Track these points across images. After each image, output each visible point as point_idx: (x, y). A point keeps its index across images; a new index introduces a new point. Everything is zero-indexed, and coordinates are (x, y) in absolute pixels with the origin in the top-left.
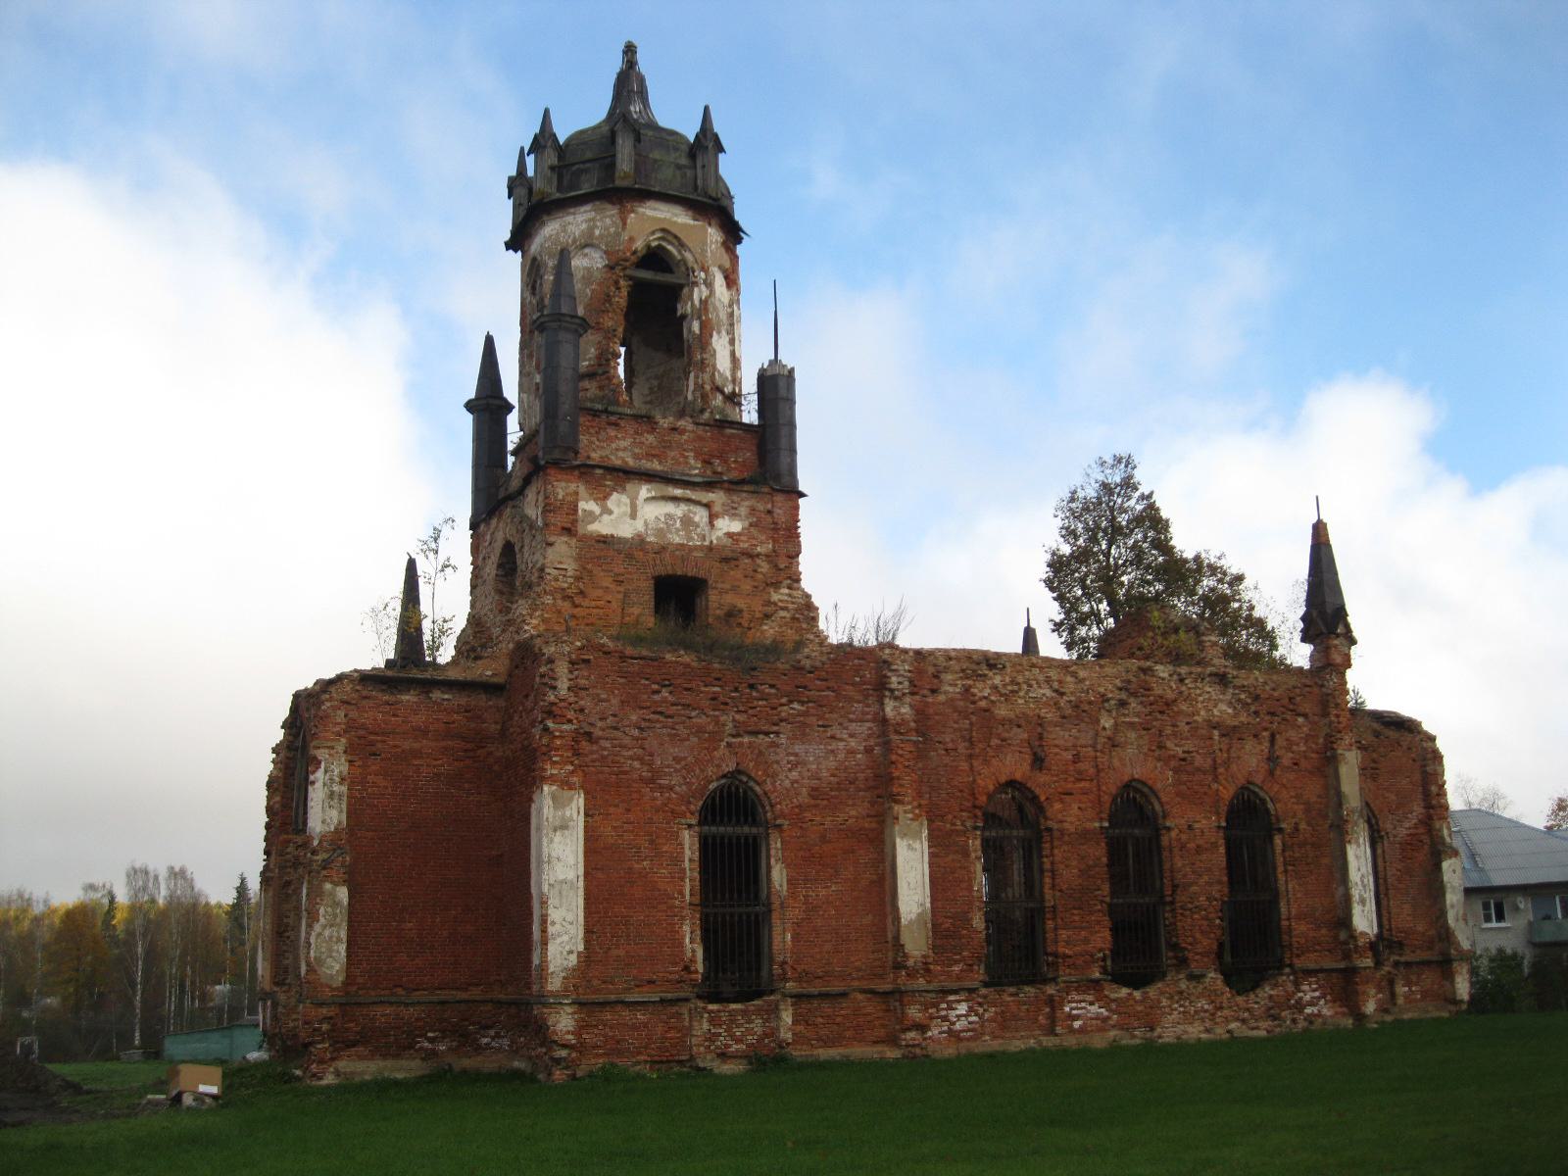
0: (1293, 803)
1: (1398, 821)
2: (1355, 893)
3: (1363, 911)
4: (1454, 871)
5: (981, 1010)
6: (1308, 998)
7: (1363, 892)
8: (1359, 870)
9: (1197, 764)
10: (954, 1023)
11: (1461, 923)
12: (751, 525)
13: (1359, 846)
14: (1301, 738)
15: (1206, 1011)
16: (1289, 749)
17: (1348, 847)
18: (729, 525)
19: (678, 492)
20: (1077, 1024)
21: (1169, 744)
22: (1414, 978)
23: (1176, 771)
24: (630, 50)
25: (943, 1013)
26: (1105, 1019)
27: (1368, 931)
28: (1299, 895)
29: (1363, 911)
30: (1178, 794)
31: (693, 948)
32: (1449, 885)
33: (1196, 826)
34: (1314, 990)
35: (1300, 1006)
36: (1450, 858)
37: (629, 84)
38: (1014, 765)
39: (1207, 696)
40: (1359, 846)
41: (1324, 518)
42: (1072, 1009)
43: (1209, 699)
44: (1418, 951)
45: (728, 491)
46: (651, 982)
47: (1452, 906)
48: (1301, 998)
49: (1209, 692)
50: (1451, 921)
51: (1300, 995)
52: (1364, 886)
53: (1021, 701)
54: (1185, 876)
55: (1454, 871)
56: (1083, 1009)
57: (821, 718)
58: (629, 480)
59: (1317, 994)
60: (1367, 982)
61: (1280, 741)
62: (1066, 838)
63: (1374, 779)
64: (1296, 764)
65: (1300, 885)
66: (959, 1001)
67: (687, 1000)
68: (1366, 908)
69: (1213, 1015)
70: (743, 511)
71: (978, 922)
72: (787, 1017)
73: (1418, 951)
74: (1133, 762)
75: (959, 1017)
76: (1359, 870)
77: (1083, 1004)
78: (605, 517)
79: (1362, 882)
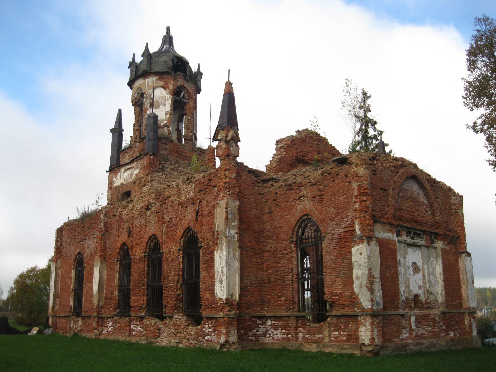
0: (208, 233)
1: (336, 225)
2: (217, 277)
3: (221, 286)
4: (361, 254)
5: (115, 325)
6: (207, 331)
7: (222, 276)
8: (221, 264)
9: (173, 223)
10: (109, 329)
11: (365, 291)
12: (141, 169)
13: (222, 251)
14: (212, 199)
15: (173, 333)
16: (207, 206)
17: (215, 252)
18: (137, 171)
19: (128, 167)
20: (134, 333)
21: (165, 217)
22: (342, 326)
23: (166, 228)
24: (168, 28)
25: (107, 325)
26: (141, 332)
27: (222, 297)
28: (206, 279)
29: (221, 286)
30: (168, 238)
31: (72, 303)
32: (356, 264)
33: (172, 250)
34: (210, 328)
35: (204, 336)
36: (358, 244)
37: (168, 40)
38: (124, 237)
39: (186, 190)
40: (222, 251)
41: (231, 81)
42: (133, 327)
43: (187, 191)
44: (346, 308)
45: (137, 161)
46: (66, 311)
47: (357, 278)
48: (204, 331)
49: (187, 188)
50: (356, 288)
51: (204, 329)
52: (223, 273)
53: (134, 212)
54: (167, 273)
55: (361, 254)
56: (136, 327)
57: (93, 232)
58: (120, 168)
59: (211, 330)
60: (222, 326)
61: (204, 203)
62: (136, 261)
63: (321, 201)
64: (210, 212)
65: (207, 274)
66: (110, 321)
67: (70, 316)
68: (223, 285)
69: (176, 335)
70: (139, 165)
71: (116, 293)
72: (80, 323)
73: (346, 308)
74: (152, 229)
75: (110, 326)
76: (221, 264)
77: (136, 326)
78: (117, 181)
79: (222, 270)
